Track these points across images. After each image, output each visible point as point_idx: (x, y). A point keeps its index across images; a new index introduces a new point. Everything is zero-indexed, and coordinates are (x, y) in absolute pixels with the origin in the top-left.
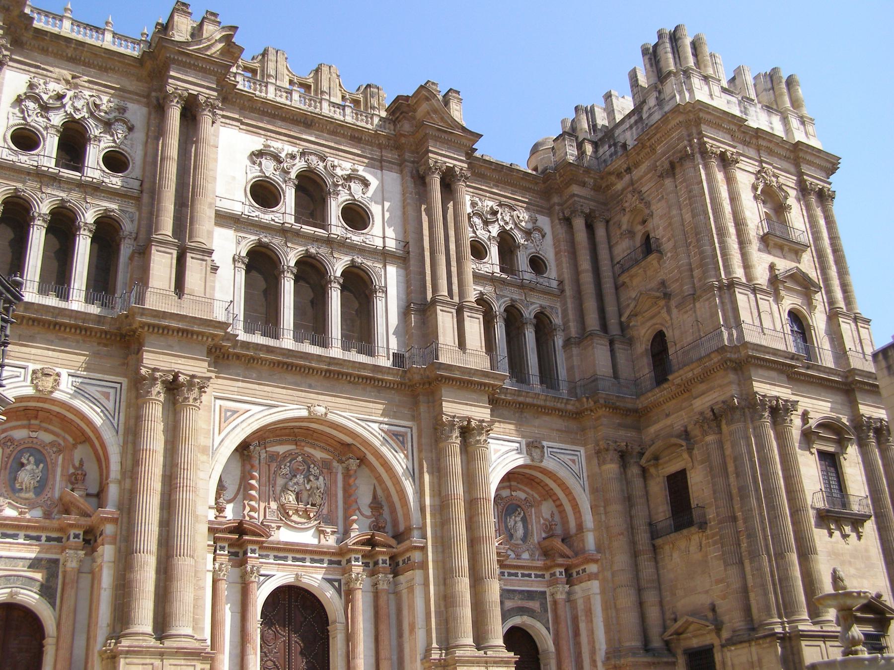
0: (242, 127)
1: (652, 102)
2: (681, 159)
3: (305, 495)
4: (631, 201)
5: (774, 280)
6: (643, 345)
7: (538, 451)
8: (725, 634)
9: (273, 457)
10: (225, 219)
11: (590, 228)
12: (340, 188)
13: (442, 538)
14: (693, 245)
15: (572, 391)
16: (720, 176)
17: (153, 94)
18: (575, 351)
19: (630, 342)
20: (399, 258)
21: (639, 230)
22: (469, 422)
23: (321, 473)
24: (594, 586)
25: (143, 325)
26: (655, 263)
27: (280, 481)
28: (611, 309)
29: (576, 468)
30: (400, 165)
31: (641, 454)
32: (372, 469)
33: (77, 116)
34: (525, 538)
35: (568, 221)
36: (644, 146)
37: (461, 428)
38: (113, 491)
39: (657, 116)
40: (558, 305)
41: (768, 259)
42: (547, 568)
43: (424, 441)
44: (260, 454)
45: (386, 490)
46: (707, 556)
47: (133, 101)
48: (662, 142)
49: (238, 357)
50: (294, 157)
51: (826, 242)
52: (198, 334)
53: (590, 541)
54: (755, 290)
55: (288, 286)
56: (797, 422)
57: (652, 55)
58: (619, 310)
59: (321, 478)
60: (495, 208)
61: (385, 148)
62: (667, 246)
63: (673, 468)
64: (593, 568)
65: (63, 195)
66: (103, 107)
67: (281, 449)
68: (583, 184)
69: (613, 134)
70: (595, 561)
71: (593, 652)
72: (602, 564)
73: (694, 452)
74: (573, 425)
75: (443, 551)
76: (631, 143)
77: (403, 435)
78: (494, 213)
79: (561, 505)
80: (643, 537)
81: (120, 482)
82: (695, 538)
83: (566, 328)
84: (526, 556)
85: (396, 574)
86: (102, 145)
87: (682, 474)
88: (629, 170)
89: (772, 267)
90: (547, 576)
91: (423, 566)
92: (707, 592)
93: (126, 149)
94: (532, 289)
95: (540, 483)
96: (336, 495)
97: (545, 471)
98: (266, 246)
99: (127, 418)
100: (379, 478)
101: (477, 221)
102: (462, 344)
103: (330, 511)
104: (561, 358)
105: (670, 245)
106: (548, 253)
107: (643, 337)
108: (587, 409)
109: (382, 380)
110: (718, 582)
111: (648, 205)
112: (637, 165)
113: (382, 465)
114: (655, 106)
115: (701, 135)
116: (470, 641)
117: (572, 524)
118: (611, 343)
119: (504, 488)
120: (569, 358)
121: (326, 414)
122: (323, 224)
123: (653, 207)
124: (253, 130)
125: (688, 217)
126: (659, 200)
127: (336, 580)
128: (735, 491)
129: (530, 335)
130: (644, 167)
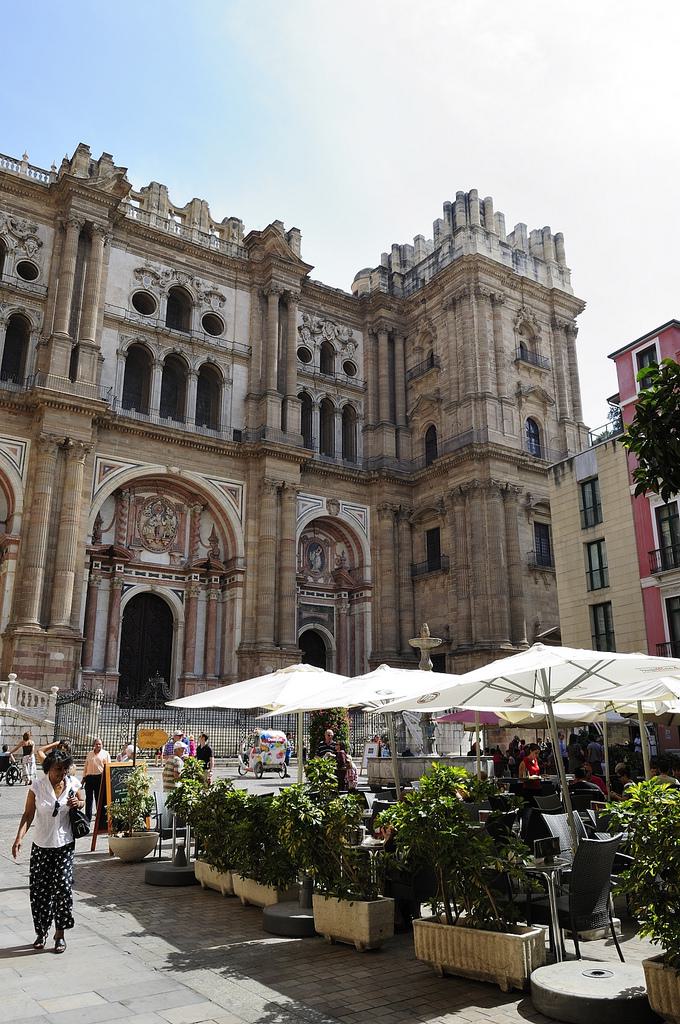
1: (446, 249)
2: (461, 297)
3: (162, 529)
4: (423, 325)
5: (519, 395)
6: (419, 435)
7: (335, 507)
8: (454, 647)
9: (139, 501)
10: (111, 321)
11: (391, 342)
13: (258, 566)
15: (365, 463)
16: (488, 311)
17: (59, 218)
18: (371, 435)
19: (412, 432)
22: (284, 484)
23: (175, 514)
24: (369, 605)
25: (44, 401)
26: (434, 374)
27: (144, 518)
28: (400, 406)
29: (362, 521)
31: (410, 514)
32: (213, 513)
34: (321, 568)
35: (375, 336)
36: (436, 284)
37: (278, 488)
38: (17, 521)
39: (447, 262)
40: (362, 401)
41: (516, 378)
42: (335, 590)
43: (250, 496)
44: (130, 499)
45: (221, 528)
47: (43, 222)
49: (116, 427)
51: (564, 368)
52: (85, 409)
53: (368, 575)
54: (501, 401)
55: (158, 375)
56: (522, 501)
57: (450, 209)
58: (406, 406)
59: (174, 518)
60: (321, 323)
62: (444, 363)
63: (431, 526)
64: (368, 593)
66: (18, 227)
67: (146, 495)
68: (390, 308)
70: (370, 589)
71: (363, 652)
74: (363, 490)
76: (427, 279)
77: (236, 491)
78: (320, 327)
79: (350, 546)
80: (406, 574)
81: (22, 515)
82: (441, 579)
83: (366, 418)
84: (321, 581)
85: (223, 589)
87: (437, 530)
88: (424, 301)
89: (519, 384)
90: (335, 597)
91: (243, 585)
92: (445, 616)
93: (35, 261)
94: (343, 387)
95: (336, 529)
96: (185, 530)
97: (340, 522)
98: (143, 344)
99: (29, 469)
100: (217, 520)
101: (306, 332)
102: (284, 427)
103: (179, 542)
104: (360, 439)
105: (447, 361)
106: (359, 359)
109: (223, 450)
110: (452, 610)
111: (434, 331)
112: (430, 298)
115: (477, 280)
116: (271, 640)
117: (357, 560)
118: (397, 431)
119: (310, 531)
120: (366, 440)
122: (187, 330)
123: (438, 332)
124: (137, 251)
125: (460, 343)
128: (469, 547)
129: (338, 421)
130: (435, 300)
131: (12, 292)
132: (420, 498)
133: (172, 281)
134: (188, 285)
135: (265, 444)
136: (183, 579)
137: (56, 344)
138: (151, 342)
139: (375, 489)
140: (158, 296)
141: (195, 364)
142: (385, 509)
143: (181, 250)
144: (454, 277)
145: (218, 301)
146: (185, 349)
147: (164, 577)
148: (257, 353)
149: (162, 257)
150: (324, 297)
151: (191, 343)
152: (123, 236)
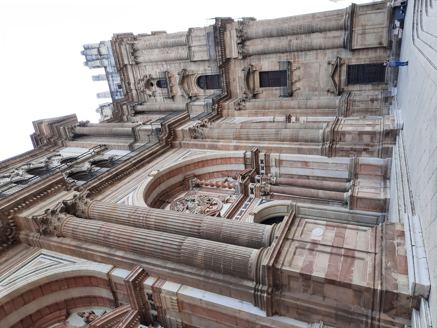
14: (168, 51)
21: (155, 88)
35: (137, 113)
46: (303, 63)
48: (123, 59)
62: (165, 68)
69: (113, 92)
72: (292, 113)
73: (254, 65)
75: (265, 140)
82: (294, 68)
87: (261, 74)
88: (129, 84)
91: (270, 150)
92: (320, 65)
105: (165, 66)
107: (198, 90)
108: (218, 109)
109: (157, 151)
110: (317, 58)
113: (203, 166)
114: (108, 61)
121: (158, 171)
126: (146, 69)
127: (262, 200)
132: (238, 91)
136: (251, 199)
139: (225, 112)
142: (239, 104)
144: (121, 54)
147: (245, 207)
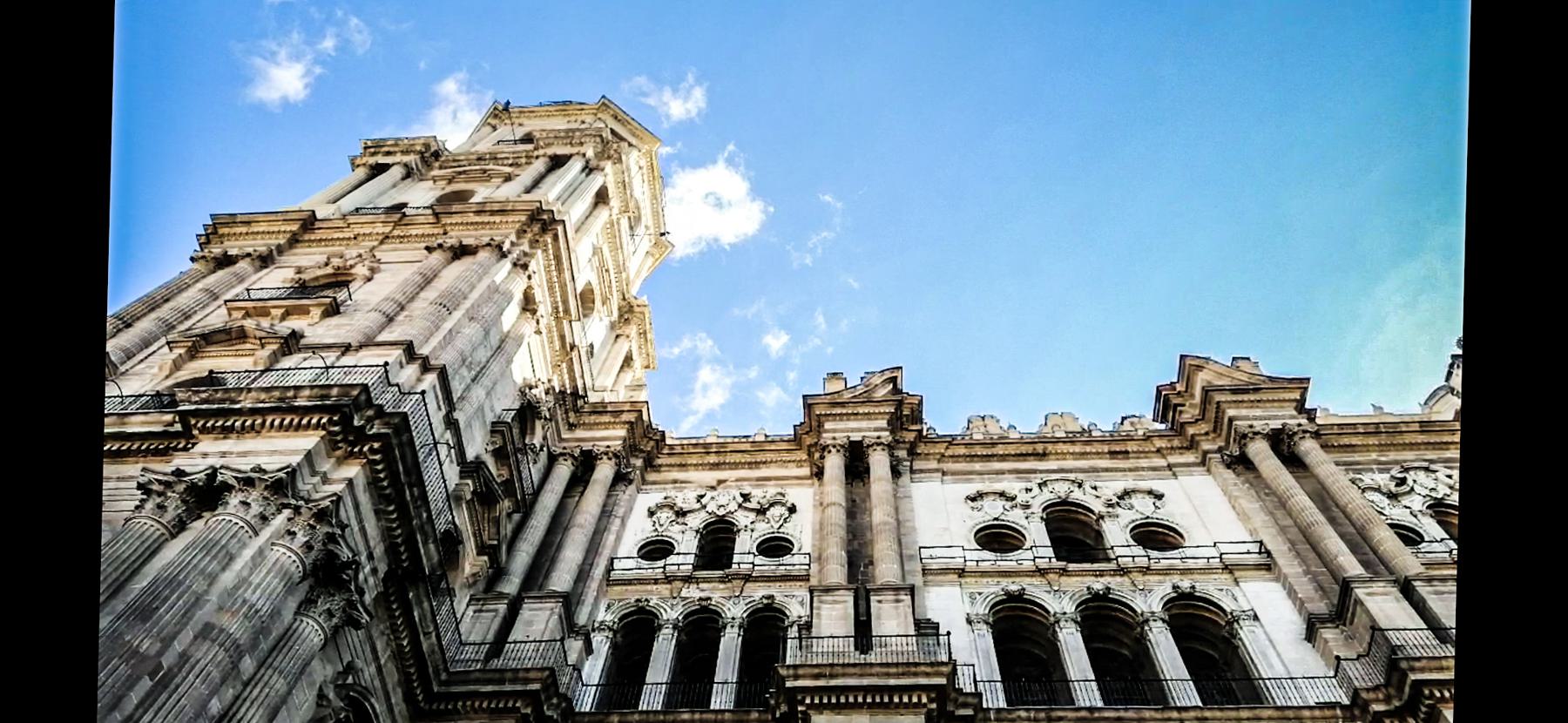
0: (945, 478)
12: (1119, 510)
20: (1258, 567)
30: (1203, 463)
33: (721, 512)
50: (1031, 490)
55: (1071, 643)
61: (1171, 454)
65: (703, 595)
86: (755, 535)
93: (790, 530)
131: (748, 578)
133: (1046, 496)
134: (1077, 495)
135: (1413, 669)
137: (821, 602)
138: (1036, 590)
140: (1024, 522)
141: (1149, 599)
143: (1043, 456)
145: (1149, 500)
146: (1120, 586)
148: (1277, 546)
149: (1011, 472)
150: (1372, 441)
151: (1123, 571)
152: (933, 465)
